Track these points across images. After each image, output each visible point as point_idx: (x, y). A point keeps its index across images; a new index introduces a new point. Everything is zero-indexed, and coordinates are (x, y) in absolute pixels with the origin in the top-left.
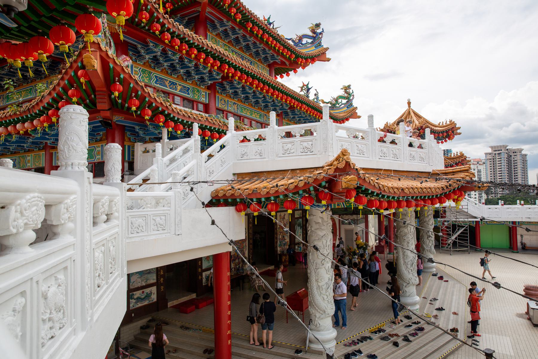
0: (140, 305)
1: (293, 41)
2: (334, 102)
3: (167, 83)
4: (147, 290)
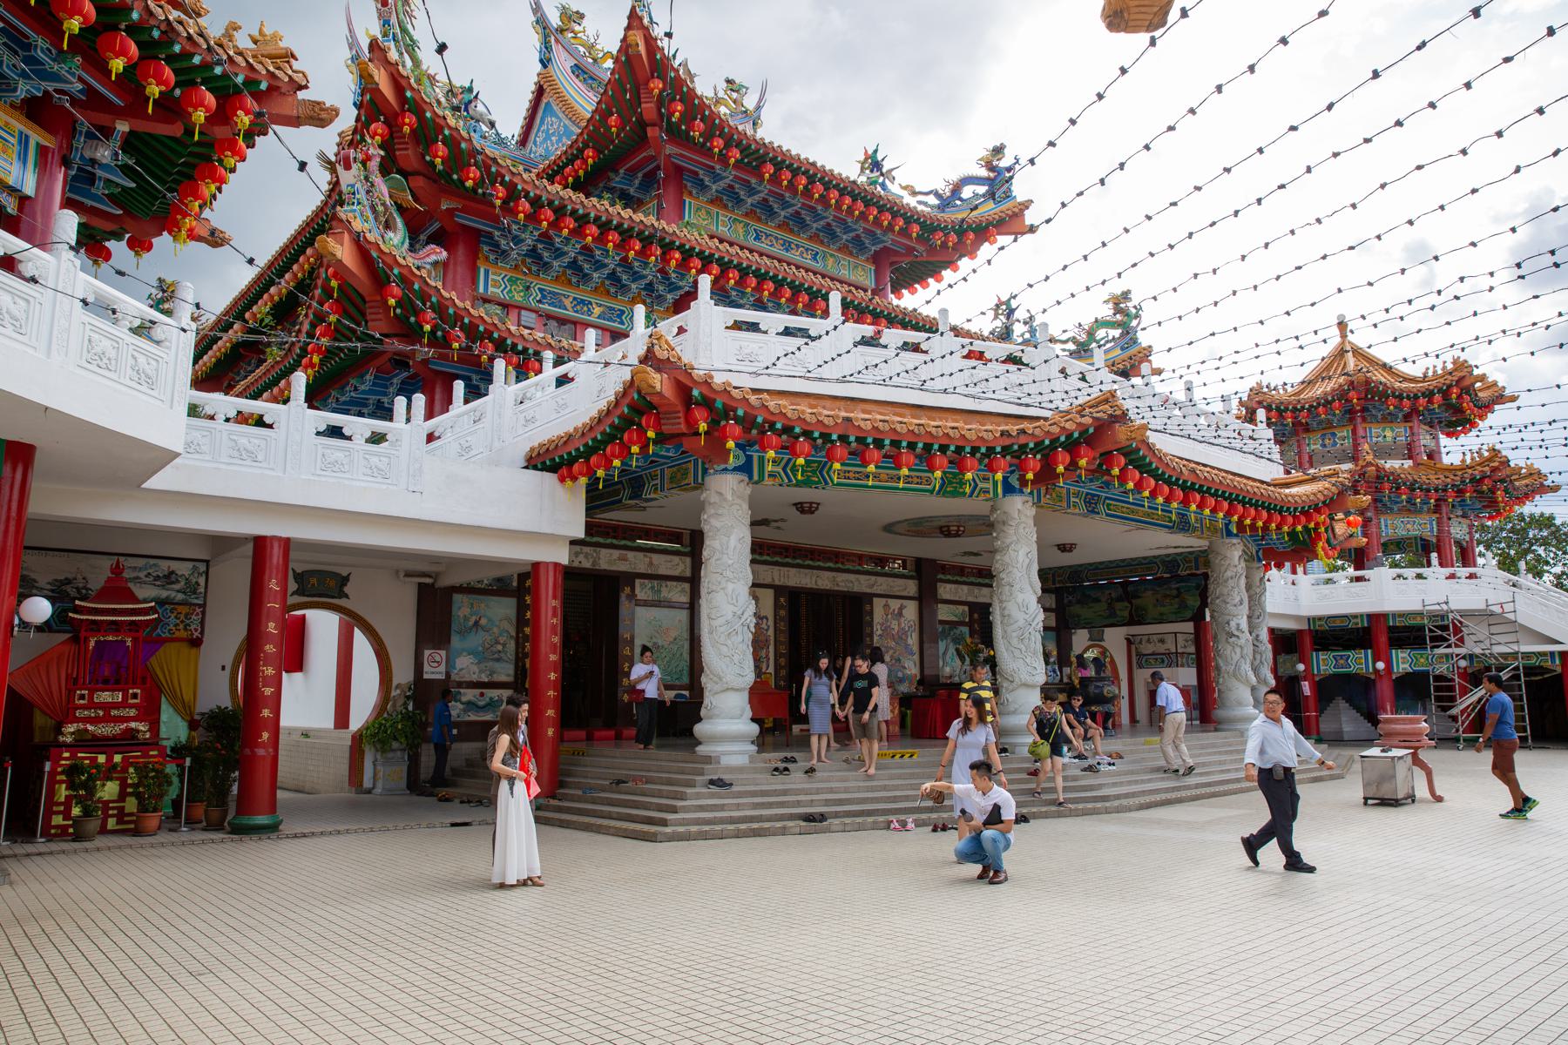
0: (473, 717)
1: (937, 195)
2: (1083, 337)
3: (567, 302)
4: (493, 694)
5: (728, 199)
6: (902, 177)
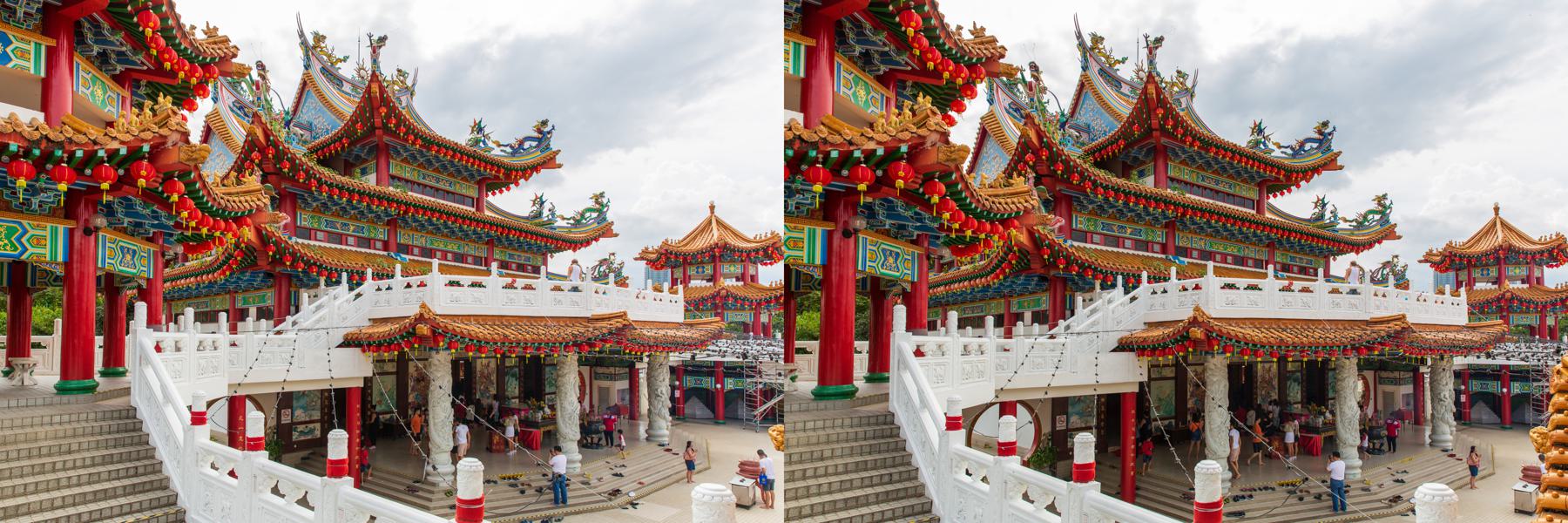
5: (411, 159)
6: (493, 137)
